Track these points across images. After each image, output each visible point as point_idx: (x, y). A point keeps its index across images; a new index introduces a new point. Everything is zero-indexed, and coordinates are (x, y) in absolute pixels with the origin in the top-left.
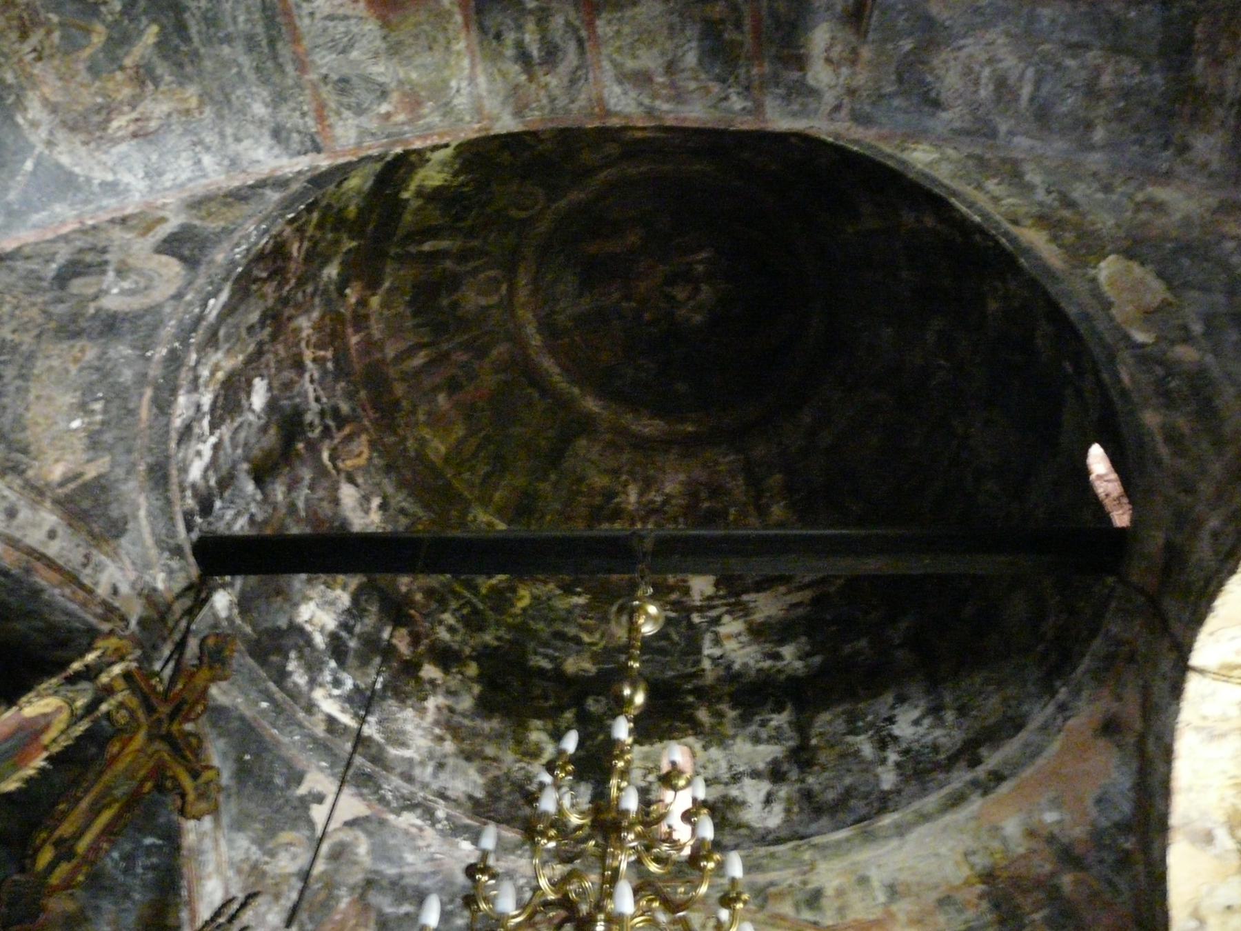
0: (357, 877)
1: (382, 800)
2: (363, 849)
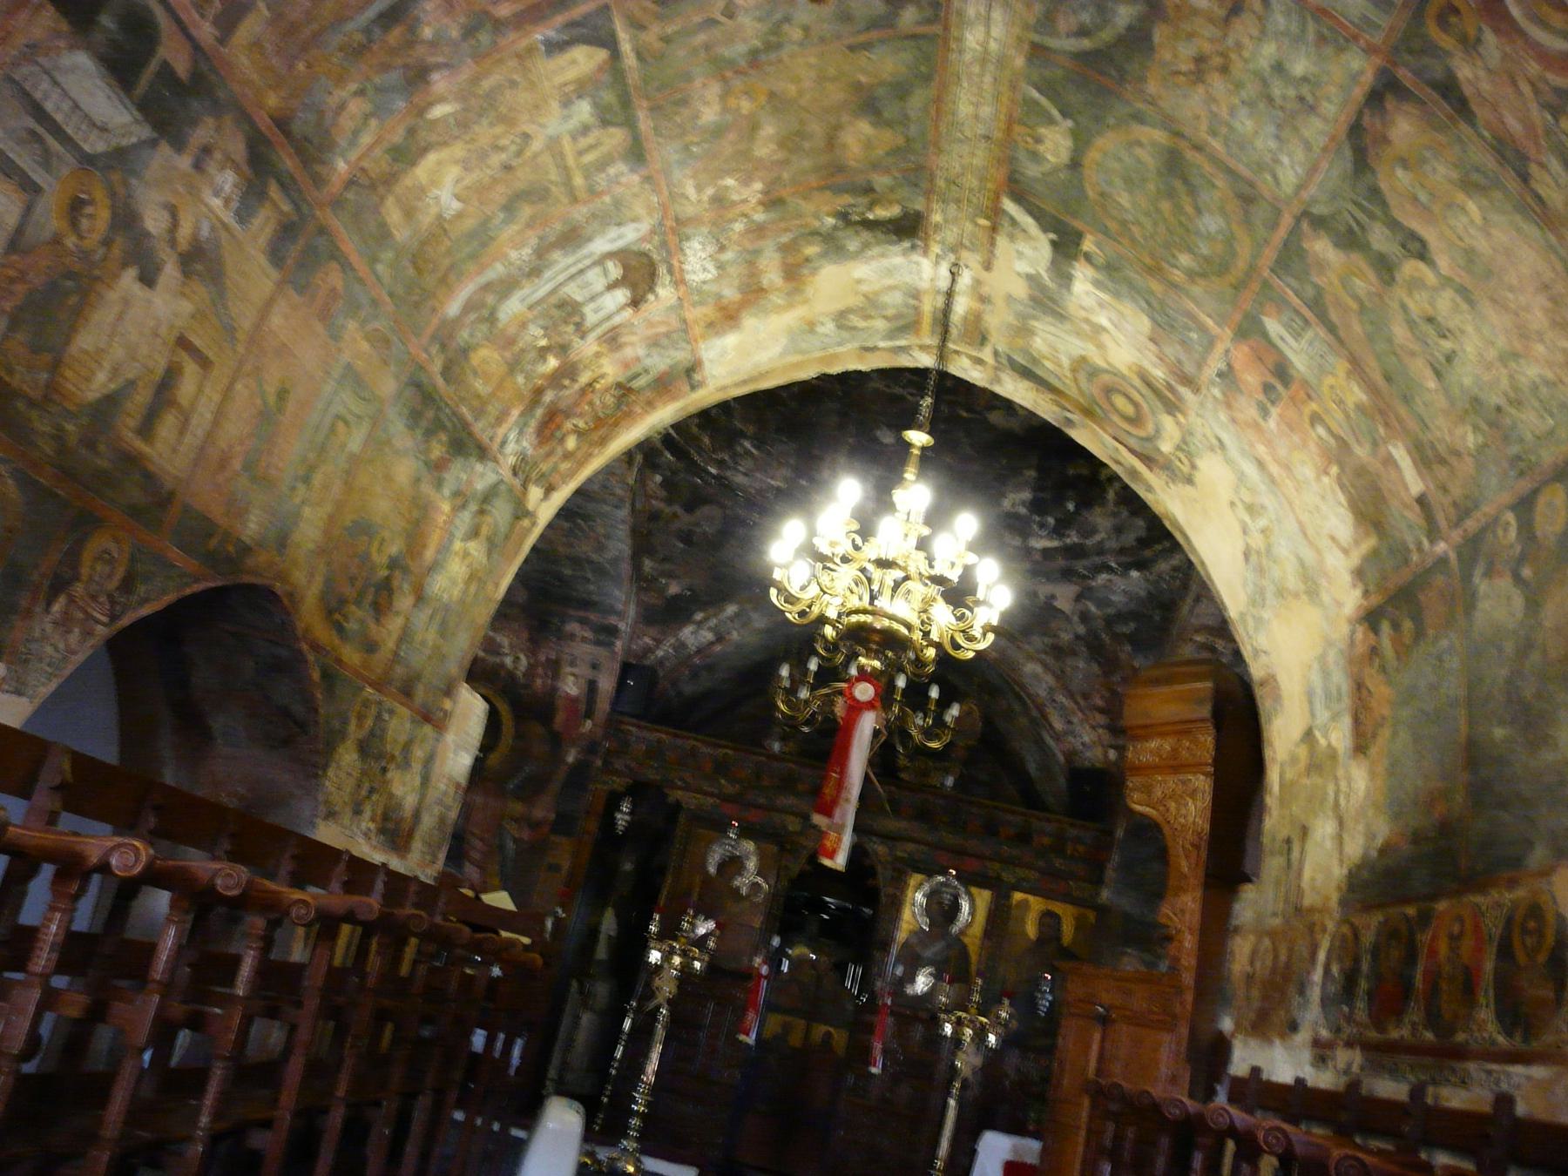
0: (1100, 624)
1: (1084, 577)
2: (1093, 609)
